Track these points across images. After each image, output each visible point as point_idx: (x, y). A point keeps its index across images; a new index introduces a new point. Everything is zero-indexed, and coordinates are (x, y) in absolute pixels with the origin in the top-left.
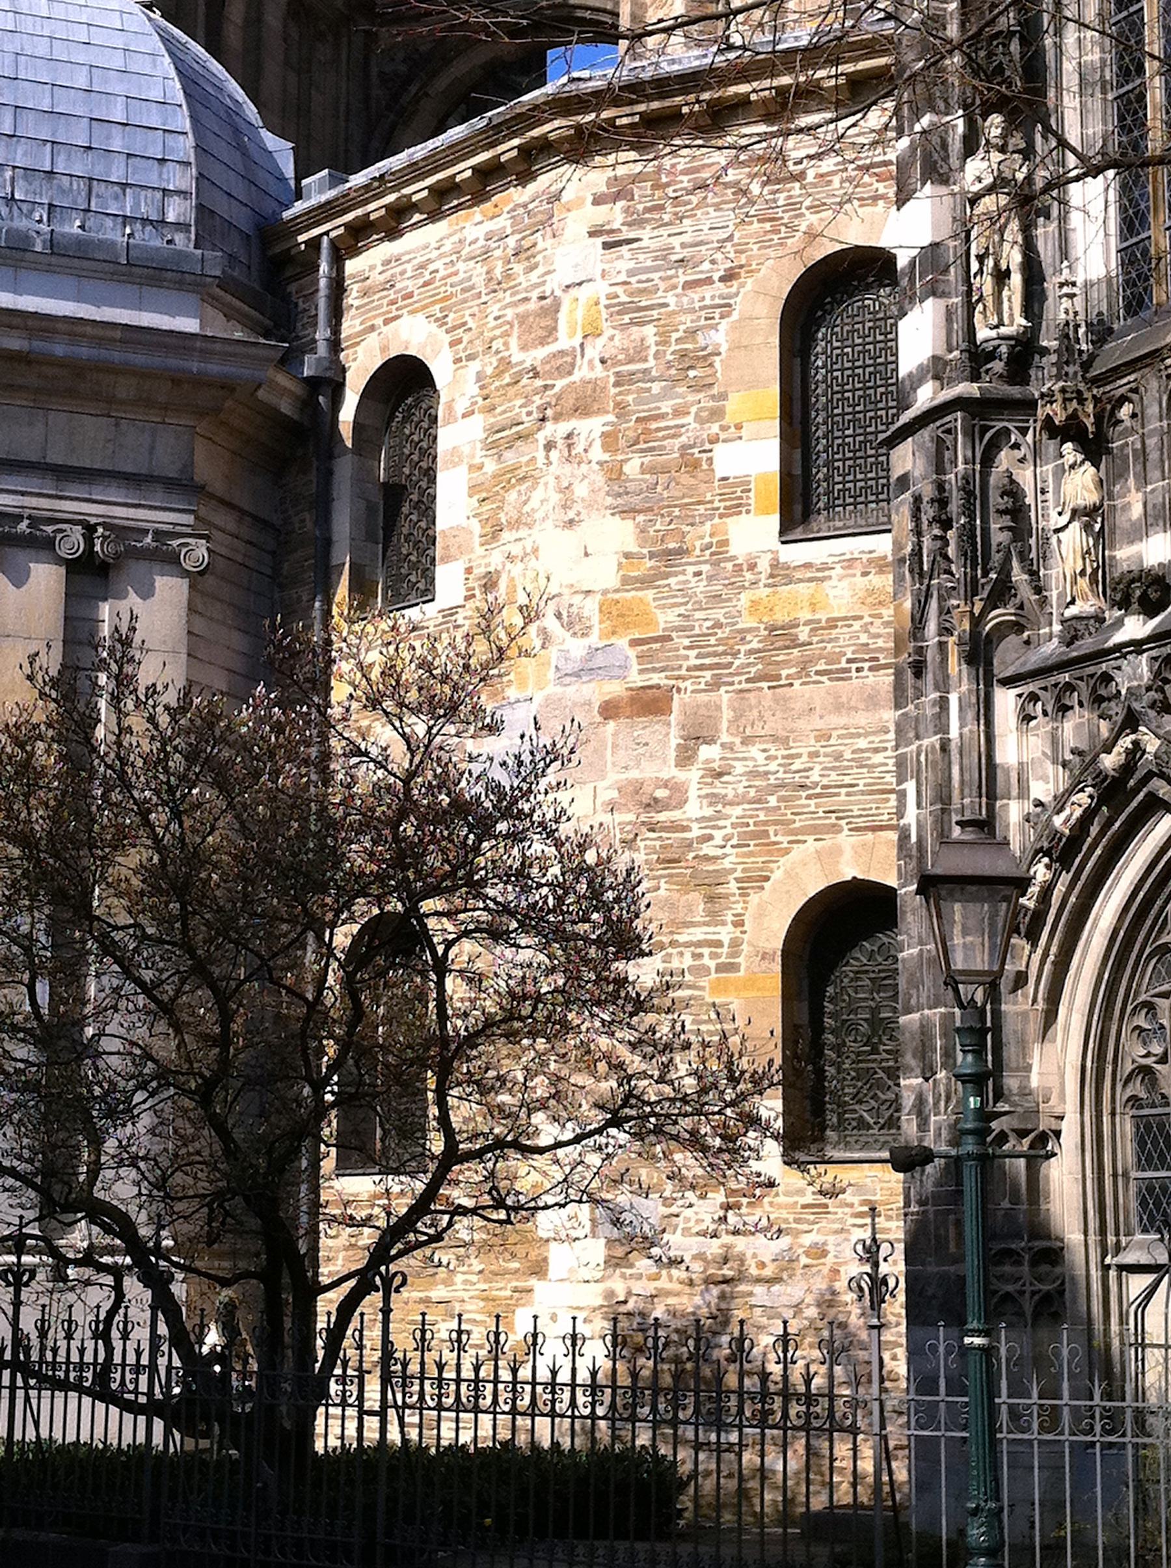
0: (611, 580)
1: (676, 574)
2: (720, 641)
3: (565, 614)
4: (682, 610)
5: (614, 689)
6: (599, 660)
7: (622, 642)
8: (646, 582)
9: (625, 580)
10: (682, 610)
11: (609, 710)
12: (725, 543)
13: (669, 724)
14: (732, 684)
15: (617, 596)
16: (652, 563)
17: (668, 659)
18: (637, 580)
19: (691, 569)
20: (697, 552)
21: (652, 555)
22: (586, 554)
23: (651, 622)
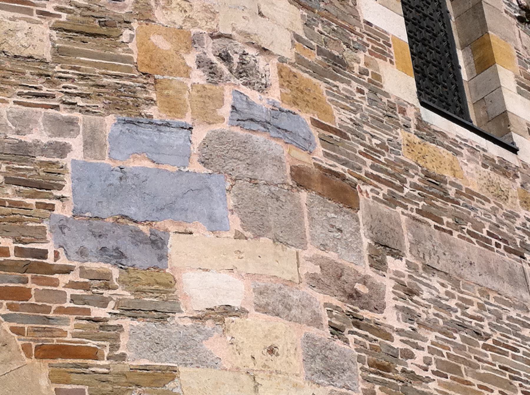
0: (289, 54)
1: (342, 81)
2: (388, 163)
3: (236, 59)
4: (353, 116)
5: (304, 159)
6: (284, 122)
7: (306, 117)
8: (318, 73)
9: (300, 61)
10: (353, 116)
11: (301, 178)
12: (378, 77)
13: (357, 220)
14: (406, 207)
15: (294, 70)
16: (320, 58)
17: (348, 155)
18: (309, 65)
19: (355, 84)
20: (356, 71)
21: (320, 52)
22: (260, 13)
23: (327, 112)
